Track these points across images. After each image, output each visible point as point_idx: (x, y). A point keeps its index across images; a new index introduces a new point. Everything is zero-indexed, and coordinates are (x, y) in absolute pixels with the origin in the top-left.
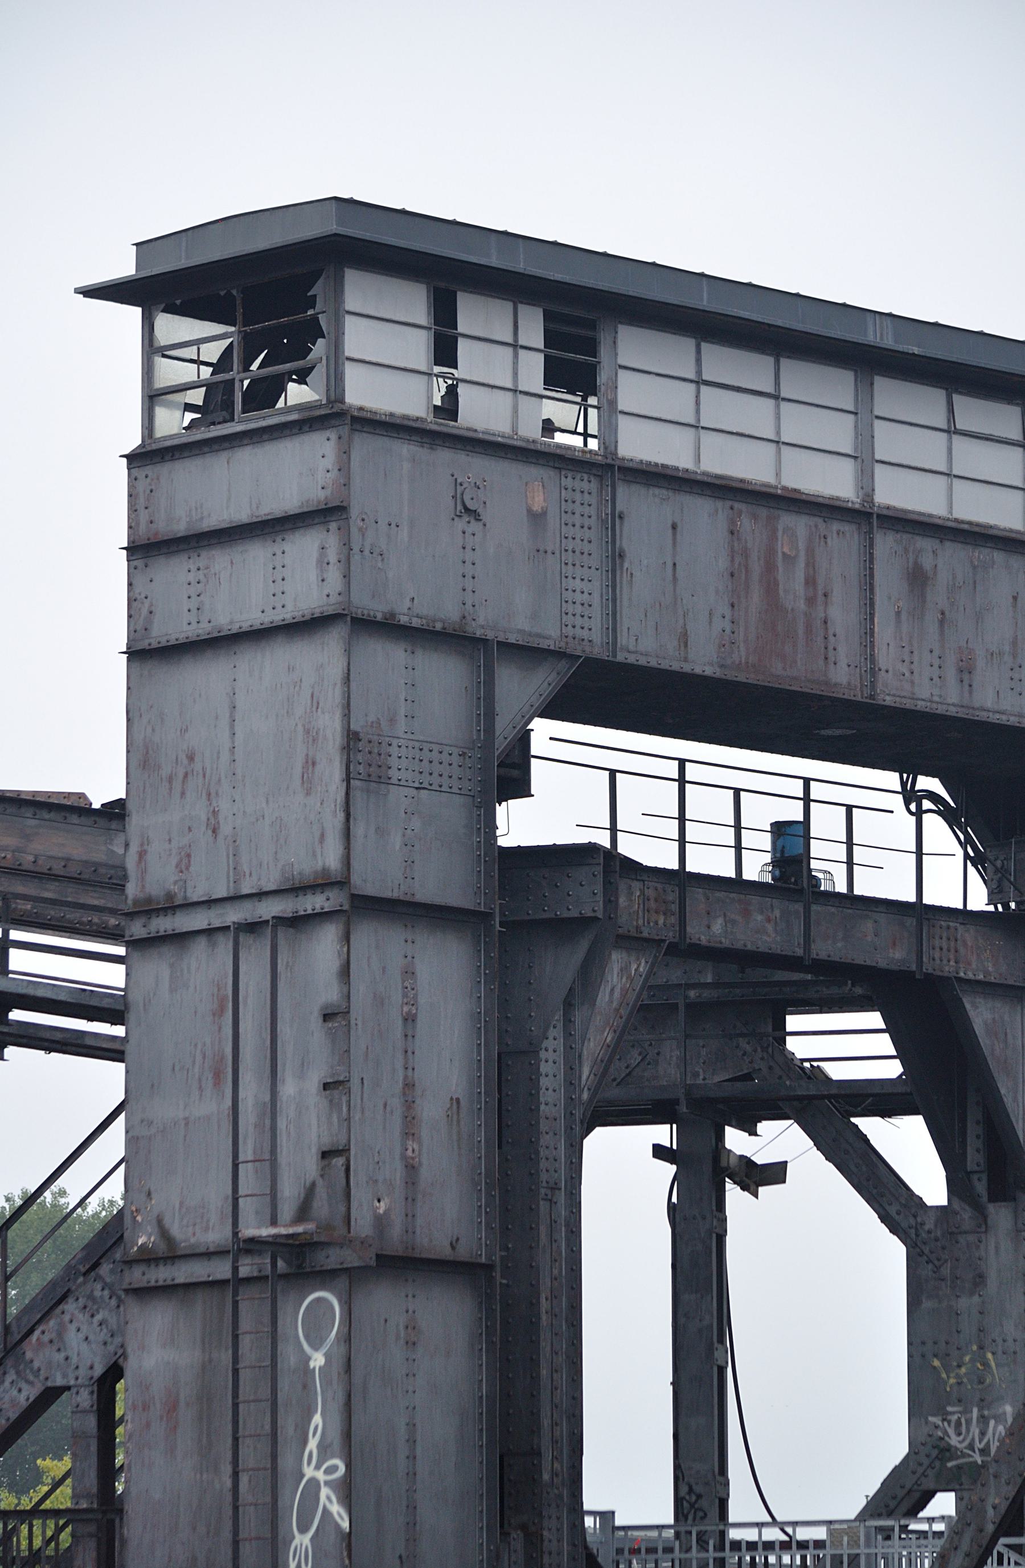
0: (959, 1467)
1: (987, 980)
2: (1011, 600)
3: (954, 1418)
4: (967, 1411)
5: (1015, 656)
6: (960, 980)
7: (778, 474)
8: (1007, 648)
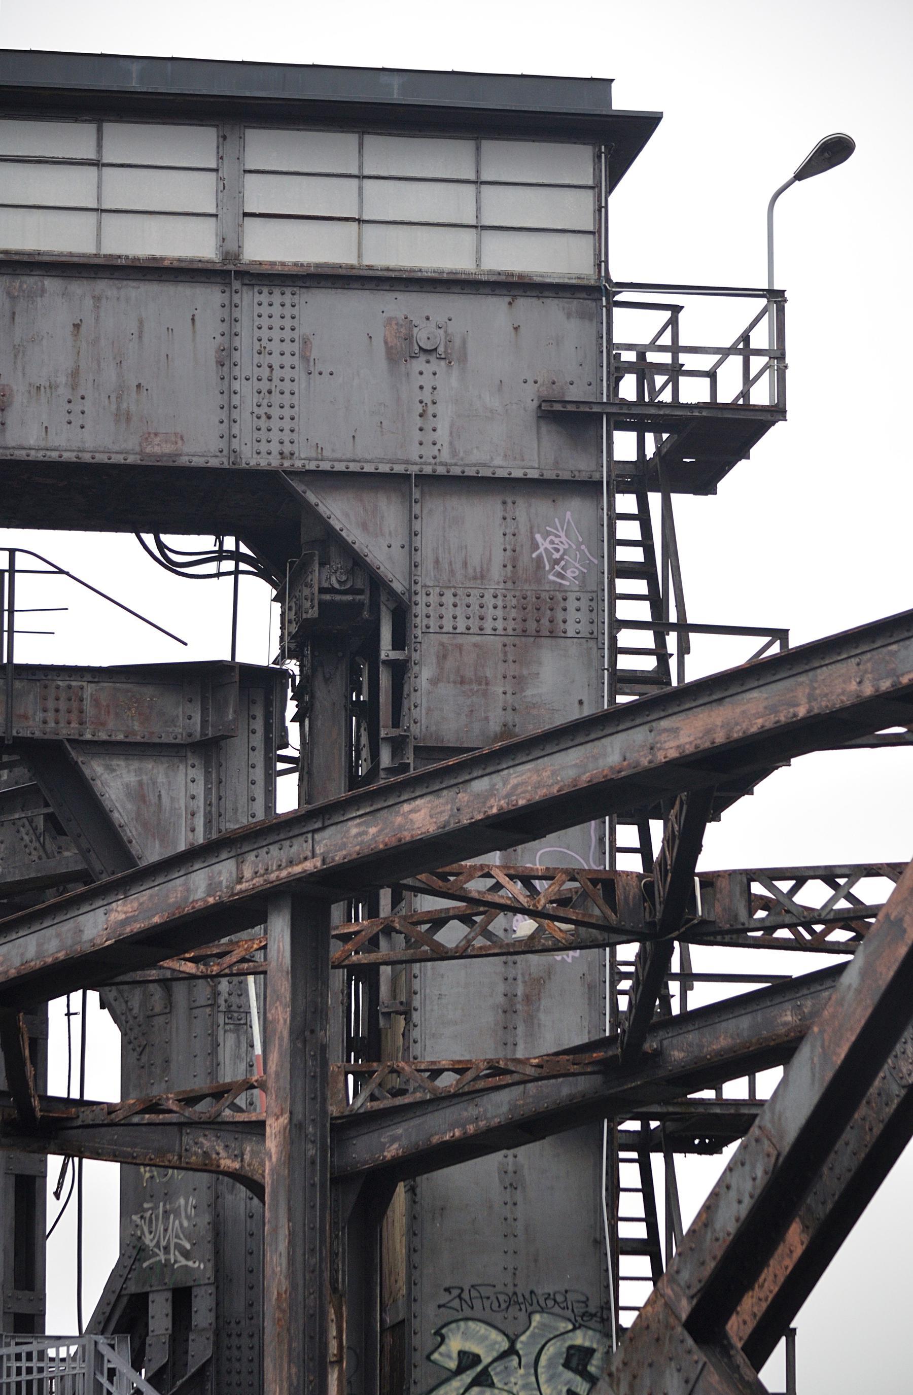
0: (151, 1268)
1: (95, 738)
2: (71, 328)
3: (148, 1215)
4: (156, 1207)
5: (74, 387)
6: (78, 743)
7: (360, 256)
8: (62, 379)
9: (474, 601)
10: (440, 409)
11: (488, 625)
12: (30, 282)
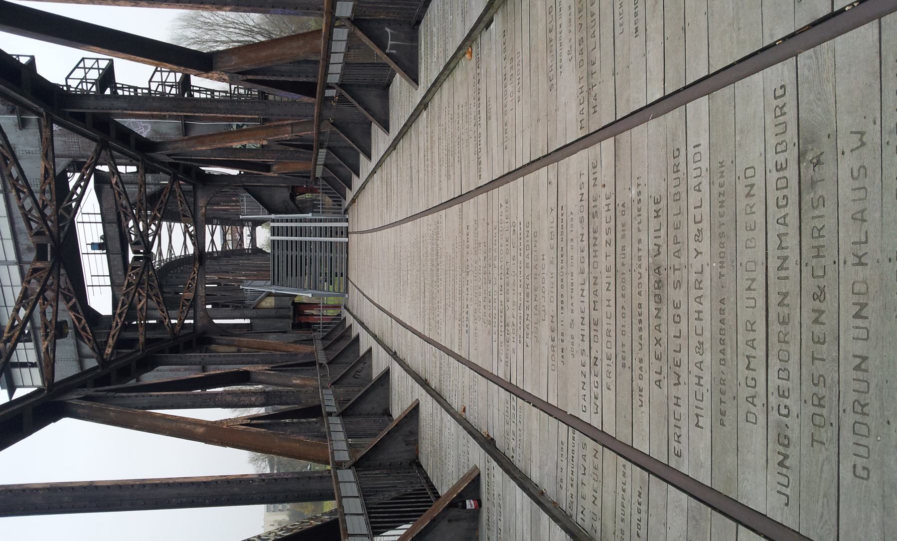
9: (71, 144)
10: (27, 150)
11: (76, 141)
12: (17, 230)
